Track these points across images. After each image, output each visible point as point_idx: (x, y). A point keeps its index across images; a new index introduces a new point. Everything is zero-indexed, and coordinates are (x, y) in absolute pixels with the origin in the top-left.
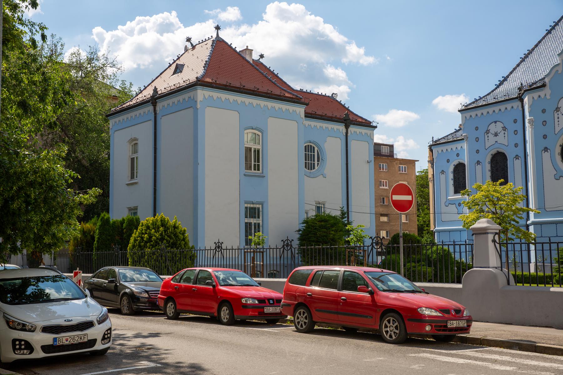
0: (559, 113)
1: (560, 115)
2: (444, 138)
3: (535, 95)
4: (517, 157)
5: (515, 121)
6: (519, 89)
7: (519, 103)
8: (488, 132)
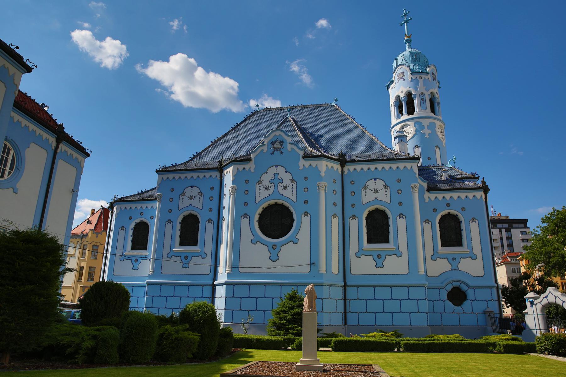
0: (261, 185)
1: (262, 188)
2: (131, 196)
3: (241, 167)
4: (210, 221)
5: (212, 188)
7: (218, 174)
8: (183, 194)
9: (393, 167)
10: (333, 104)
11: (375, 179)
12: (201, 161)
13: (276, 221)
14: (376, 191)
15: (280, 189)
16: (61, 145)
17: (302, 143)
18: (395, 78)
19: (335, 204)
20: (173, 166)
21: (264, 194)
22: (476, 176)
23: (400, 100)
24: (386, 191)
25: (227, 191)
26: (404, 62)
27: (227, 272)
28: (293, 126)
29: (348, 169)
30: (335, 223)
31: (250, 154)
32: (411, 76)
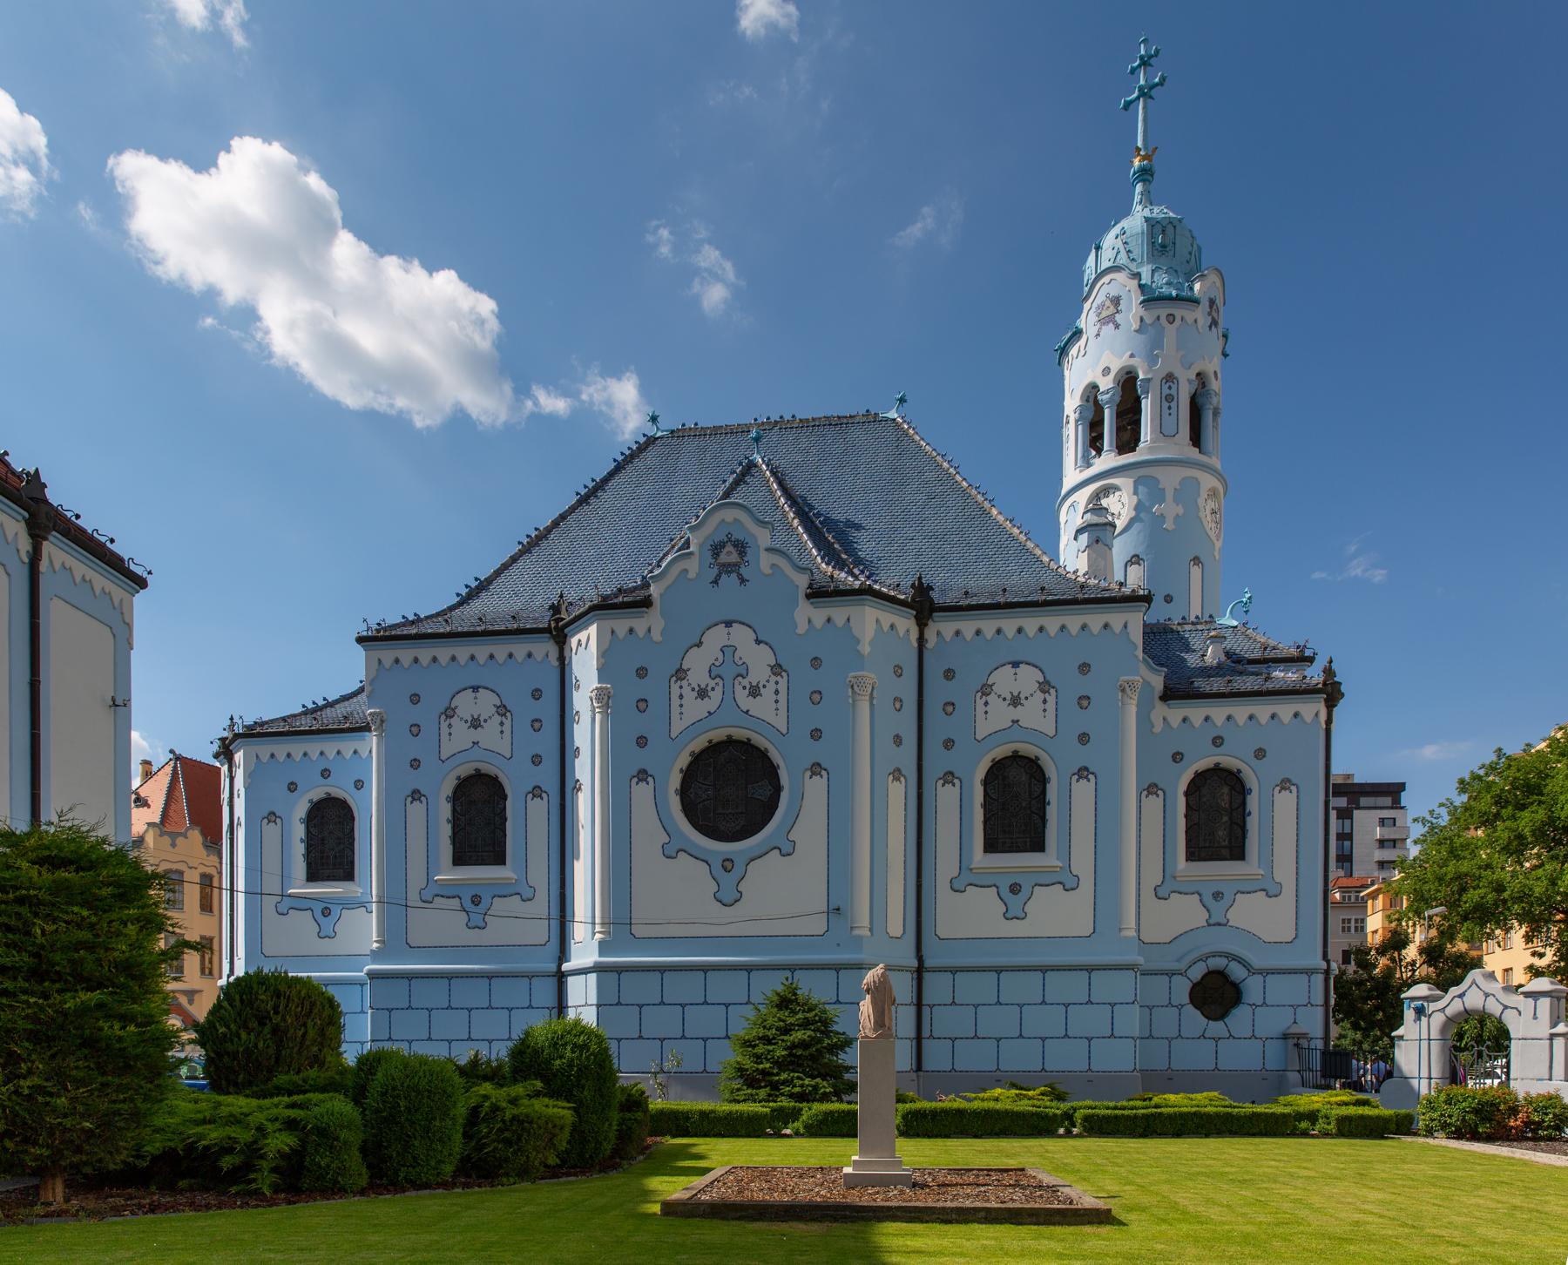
0: (684, 683)
1: (686, 691)
5: (537, 694)
6: (552, 607)
7: (550, 648)
8: (449, 712)
9: (1069, 626)
10: (893, 414)
11: (1016, 665)
12: (493, 606)
13: (730, 791)
14: (1015, 701)
15: (742, 695)
16: (47, 547)
17: (802, 548)
18: (1087, 320)
19: (898, 740)
20: (407, 623)
21: (696, 710)
22: (1308, 653)
23: (1096, 401)
24: (1045, 701)
25: (583, 700)
26: (1123, 259)
27: (598, 936)
28: (771, 492)
29: (939, 633)
30: (898, 795)
31: (646, 585)
32: (1141, 311)
